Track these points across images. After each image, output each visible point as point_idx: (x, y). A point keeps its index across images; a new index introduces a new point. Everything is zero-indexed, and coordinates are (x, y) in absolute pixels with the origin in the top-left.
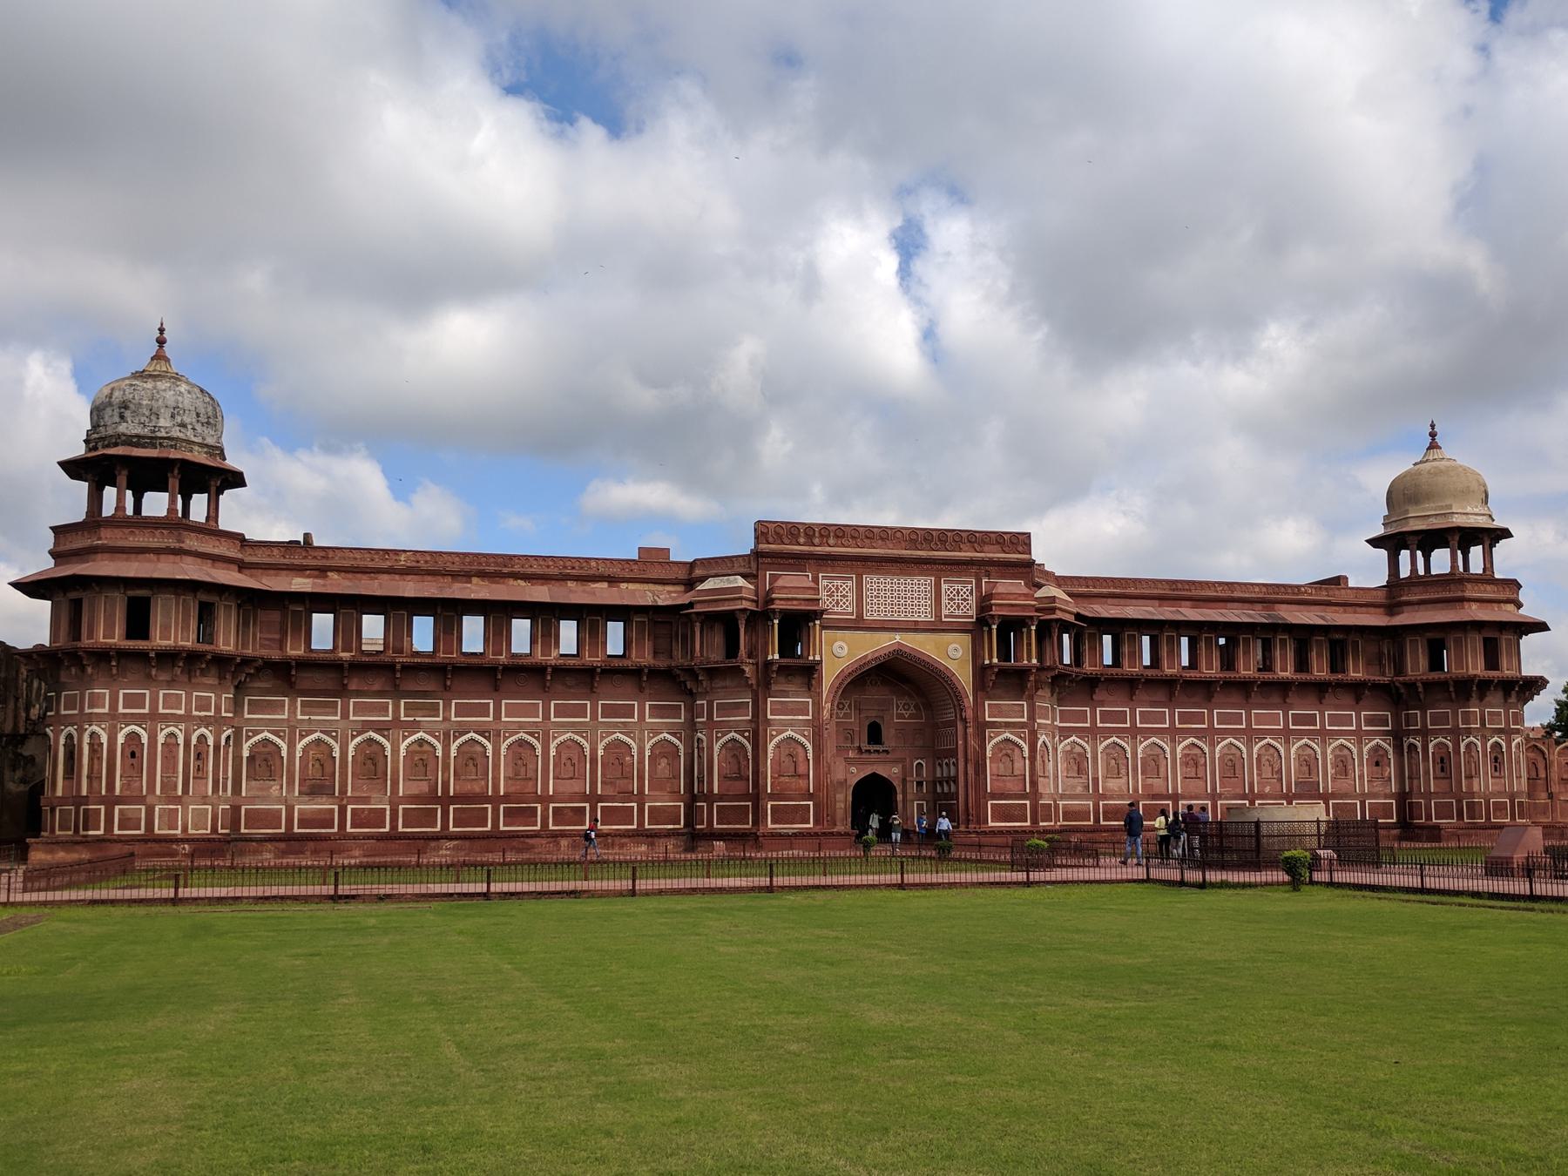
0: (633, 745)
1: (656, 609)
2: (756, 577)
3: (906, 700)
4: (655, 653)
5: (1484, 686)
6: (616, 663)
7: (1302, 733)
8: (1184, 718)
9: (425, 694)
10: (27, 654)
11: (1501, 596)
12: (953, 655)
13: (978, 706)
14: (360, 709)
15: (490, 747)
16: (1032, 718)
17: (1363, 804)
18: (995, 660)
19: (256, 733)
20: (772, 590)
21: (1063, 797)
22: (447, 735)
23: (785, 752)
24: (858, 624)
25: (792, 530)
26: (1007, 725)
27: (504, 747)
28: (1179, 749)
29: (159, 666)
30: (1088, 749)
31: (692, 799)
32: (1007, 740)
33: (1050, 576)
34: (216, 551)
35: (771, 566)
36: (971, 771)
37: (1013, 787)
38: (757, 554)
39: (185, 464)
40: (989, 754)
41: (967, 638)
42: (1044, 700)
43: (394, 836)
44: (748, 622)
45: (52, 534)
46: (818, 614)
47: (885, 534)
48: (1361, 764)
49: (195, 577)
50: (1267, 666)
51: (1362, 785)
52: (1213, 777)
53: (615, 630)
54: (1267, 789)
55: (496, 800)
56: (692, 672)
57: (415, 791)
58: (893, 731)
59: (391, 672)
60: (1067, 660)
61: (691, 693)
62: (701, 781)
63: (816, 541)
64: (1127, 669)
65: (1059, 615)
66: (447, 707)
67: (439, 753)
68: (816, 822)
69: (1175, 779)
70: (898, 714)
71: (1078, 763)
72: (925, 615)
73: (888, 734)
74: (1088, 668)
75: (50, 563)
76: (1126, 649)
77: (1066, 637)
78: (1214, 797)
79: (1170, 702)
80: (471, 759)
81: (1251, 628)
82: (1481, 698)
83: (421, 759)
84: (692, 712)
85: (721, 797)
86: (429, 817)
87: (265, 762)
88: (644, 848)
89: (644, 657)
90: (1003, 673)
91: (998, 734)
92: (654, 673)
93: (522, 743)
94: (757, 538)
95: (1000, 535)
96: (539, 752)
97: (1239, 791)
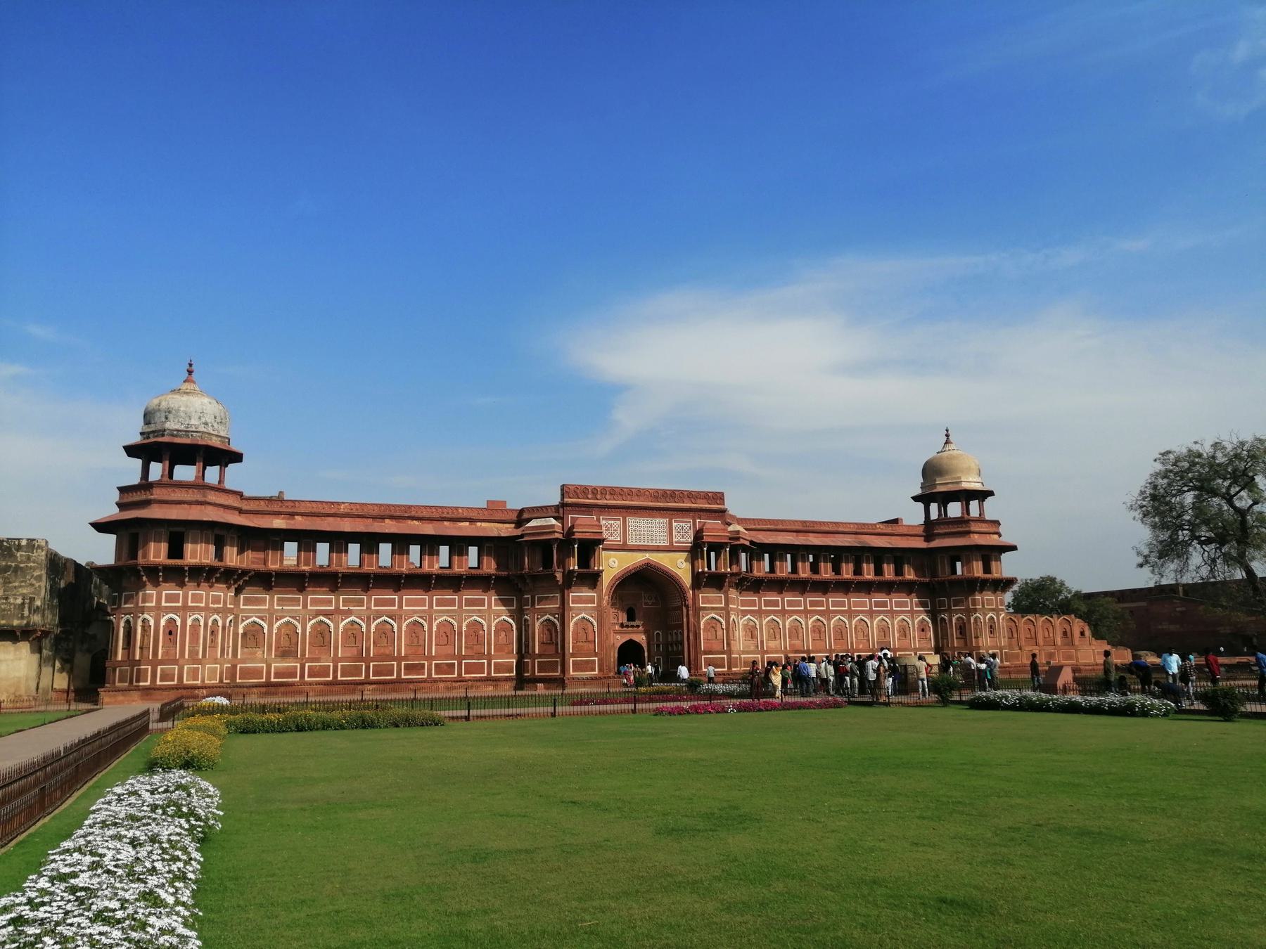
1: (499, 538)
4: (499, 567)
6: (473, 571)
8: (813, 604)
10: (103, 571)
12: (679, 566)
13: (695, 598)
14: (314, 602)
16: (727, 604)
19: (247, 618)
20: (573, 527)
21: (744, 652)
22: (369, 618)
24: (624, 548)
25: (584, 490)
26: (713, 609)
27: (404, 626)
29: (192, 578)
31: (521, 656)
33: (733, 517)
34: (226, 503)
35: (571, 512)
37: (717, 647)
38: (563, 505)
42: (733, 593)
43: (335, 683)
46: (601, 541)
47: (639, 493)
49: (215, 519)
50: (858, 571)
53: (473, 551)
55: (399, 659)
56: (522, 577)
59: (331, 580)
60: (744, 569)
61: (520, 590)
62: (527, 646)
64: (779, 574)
65: (742, 541)
67: (364, 629)
68: (600, 670)
69: (808, 642)
71: (752, 632)
73: (638, 614)
74: (756, 573)
75: (117, 510)
76: (778, 563)
77: (743, 555)
79: (803, 593)
80: (385, 634)
82: (981, 591)
83: (353, 634)
85: (540, 656)
86: (357, 671)
87: (253, 636)
88: (491, 688)
92: (498, 578)
93: (416, 623)
94: (563, 496)
95: (707, 493)
96: (426, 628)
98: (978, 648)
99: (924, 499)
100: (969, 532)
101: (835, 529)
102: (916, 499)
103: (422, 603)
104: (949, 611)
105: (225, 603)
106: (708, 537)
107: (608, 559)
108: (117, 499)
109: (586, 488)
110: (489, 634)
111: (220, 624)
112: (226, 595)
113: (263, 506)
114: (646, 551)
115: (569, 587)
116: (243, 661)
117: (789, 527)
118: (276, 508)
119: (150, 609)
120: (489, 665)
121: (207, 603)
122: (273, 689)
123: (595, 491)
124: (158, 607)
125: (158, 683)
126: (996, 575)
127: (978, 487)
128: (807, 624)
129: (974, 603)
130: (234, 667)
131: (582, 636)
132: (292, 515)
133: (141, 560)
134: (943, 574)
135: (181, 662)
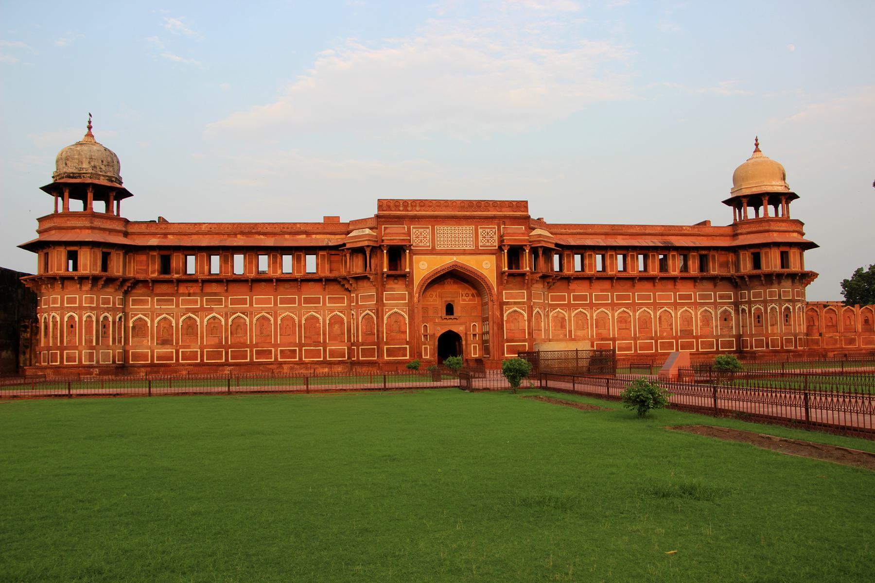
0: (321, 318)
2: (377, 228)
3: (467, 291)
4: (331, 271)
5: (779, 276)
6: (310, 276)
7: (684, 304)
8: (619, 298)
9: (215, 294)
11: (791, 229)
12: (486, 267)
13: (500, 293)
14: (185, 302)
15: (248, 320)
16: (529, 298)
17: (717, 341)
18: (506, 269)
19: (136, 315)
22: (226, 314)
23: (393, 319)
24: (433, 252)
25: (397, 203)
26: (515, 303)
28: (616, 314)
30: (567, 315)
32: (515, 311)
34: (110, 227)
36: (495, 328)
37: (518, 336)
38: (378, 217)
39: (95, 186)
40: (505, 319)
41: (494, 257)
42: (538, 288)
43: (202, 364)
44: (371, 251)
45: (37, 223)
47: (446, 204)
48: (716, 320)
51: (717, 331)
52: (634, 328)
54: (665, 334)
55: (251, 346)
56: (345, 279)
57: (213, 343)
58: (459, 308)
63: (409, 209)
64: (588, 272)
66: (226, 300)
68: (410, 355)
69: (613, 330)
70: (463, 299)
72: (470, 247)
74: (566, 272)
76: (587, 262)
78: (635, 339)
80: (238, 326)
81: (655, 249)
82: (779, 283)
83: (214, 327)
84: (350, 300)
86: (219, 355)
87: (140, 329)
88: (326, 370)
89: (327, 273)
90: (510, 275)
91: (510, 308)
92: (329, 281)
93: (263, 318)
95: (511, 202)
97: (649, 335)
98: (773, 334)
99: (735, 202)
100: (768, 231)
101: (643, 231)
102: (728, 202)
103: (268, 301)
104: (749, 303)
105: (114, 303)
106: (509, 240)
107: (418, 263)
108: (37, 228)
109: (397, 201)
110: (324, 326)
111: (111, 319)
112: (114, 298)
113: (143, 229)
114: (453, 254)
115: (383, 285)
116: (134, 347)
117: (598, 231)
118: (153, 230)
119: (55, 309)
120: (325, 351)
121: (98, 304)
122: (155, 369)
123: (406, 203)
124: (62, 307)
125: (65, 363)
126: (794, 268)
127: (781, 189)
128: (613, 316)
129: (771, 294)
130: (126, 353)
131: (395, 327)
132: (165, 235)
133: (50, 273)
134: (746, 266)
135: (80, 348)
